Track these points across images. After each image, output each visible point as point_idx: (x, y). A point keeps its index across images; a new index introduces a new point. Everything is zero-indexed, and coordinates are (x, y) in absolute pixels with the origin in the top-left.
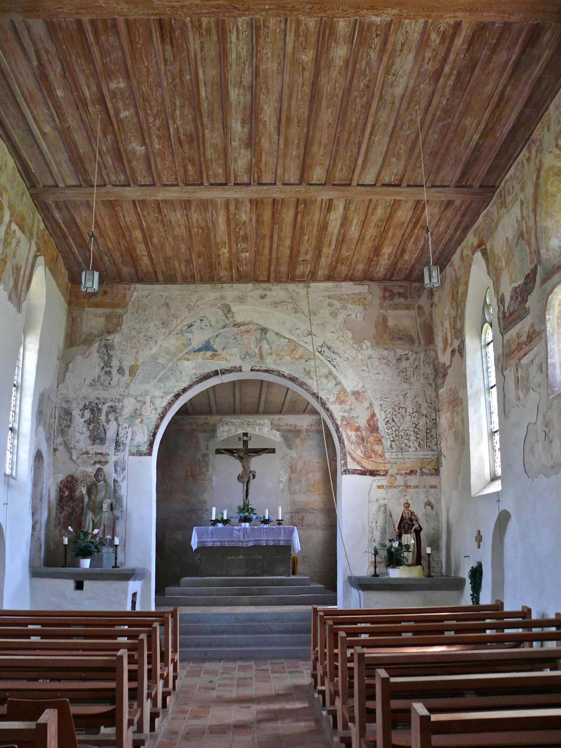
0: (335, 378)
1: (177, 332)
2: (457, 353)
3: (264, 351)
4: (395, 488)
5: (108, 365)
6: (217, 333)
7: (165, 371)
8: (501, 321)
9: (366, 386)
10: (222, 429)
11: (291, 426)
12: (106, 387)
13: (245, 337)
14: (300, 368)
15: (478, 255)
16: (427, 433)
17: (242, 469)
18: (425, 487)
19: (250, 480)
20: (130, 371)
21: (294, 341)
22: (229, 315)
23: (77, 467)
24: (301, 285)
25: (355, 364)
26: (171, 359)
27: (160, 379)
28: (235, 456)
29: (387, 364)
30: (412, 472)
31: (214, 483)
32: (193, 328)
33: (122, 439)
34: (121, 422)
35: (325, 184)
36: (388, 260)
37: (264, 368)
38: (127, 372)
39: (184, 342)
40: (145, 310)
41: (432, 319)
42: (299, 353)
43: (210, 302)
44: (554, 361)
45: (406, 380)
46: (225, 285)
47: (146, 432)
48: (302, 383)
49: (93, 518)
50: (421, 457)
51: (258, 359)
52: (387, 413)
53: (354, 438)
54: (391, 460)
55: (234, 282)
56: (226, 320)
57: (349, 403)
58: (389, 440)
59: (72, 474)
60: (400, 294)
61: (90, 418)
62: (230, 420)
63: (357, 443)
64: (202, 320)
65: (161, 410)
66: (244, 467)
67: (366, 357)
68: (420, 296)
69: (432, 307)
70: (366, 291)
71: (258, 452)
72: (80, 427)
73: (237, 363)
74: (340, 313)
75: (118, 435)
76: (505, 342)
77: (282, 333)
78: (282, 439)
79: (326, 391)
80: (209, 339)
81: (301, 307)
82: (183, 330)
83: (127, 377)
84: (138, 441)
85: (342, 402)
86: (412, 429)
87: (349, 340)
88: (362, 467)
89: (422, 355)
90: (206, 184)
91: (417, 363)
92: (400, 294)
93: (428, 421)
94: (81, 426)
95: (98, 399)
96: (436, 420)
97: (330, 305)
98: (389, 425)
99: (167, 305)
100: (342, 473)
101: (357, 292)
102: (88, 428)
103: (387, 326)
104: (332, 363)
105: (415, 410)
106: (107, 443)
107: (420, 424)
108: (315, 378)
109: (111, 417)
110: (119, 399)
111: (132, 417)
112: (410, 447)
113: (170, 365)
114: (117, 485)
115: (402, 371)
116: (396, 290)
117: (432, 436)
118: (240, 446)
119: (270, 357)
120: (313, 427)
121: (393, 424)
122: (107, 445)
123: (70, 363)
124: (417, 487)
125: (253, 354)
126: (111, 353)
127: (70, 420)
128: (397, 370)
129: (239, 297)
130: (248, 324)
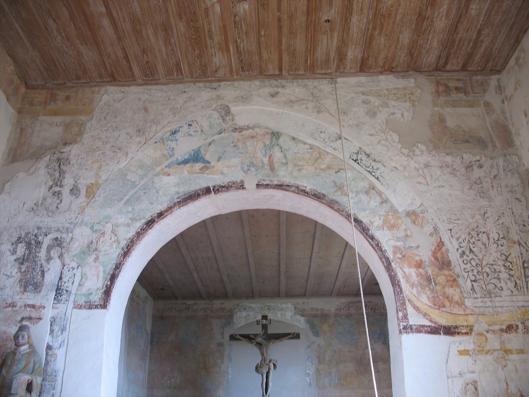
0: (380, 194)
1: (156, 140)
4: (487, 353)
5: (59, 183)
6: (210, 140)
7: (135, 190)
10: (239, 314)
11: (317, 310)
13: (248, 143)
22: (227, 118)
24: (325, 81)
27: (128, 201)
29: (454, 172)
30: (510, 328)
31: (230, 376)
32: (178, 135)
33: (67, 284)
34: (67, 260)
36: (447, 16)
37: (276, 183)
38: (83, 192)
39: (165, 152)
41: (506, 118)
45: (482, 194)
46: (222, 83)
47: (101, 274)
48: (331, 201)
50: (521, 304)
52: (461, 240)
53: (414, 278)
54: (474, 309)
55: (235, 77)
56: (224, 125)
57: (403, 227)
58: (469, 280)
60: (457, 89)
61: (24, 255)
62: (248, 305)
63: (421, 285)
65: (125, 242)
66: (262, 354)
68: (485, 91)
69: (503, 102)
71: (278, 337)
73: (237, 176)
74: (380, 112)
75: (61, 278)
77: (301, 138)
78: (308, 326)
79: (368, 212)
80: (200, 147)
81: (326, 106)
82: (164, 137)
83: (82, 199)
84: (88, 288)
85: (392, 227)
86: (501, 263)
87: (395, 144)
88: (431, 321)
89: (501, 161)
91: (494, 172)
92: (457, 89)
94: (10, 265)
95: (39, 228)
98: (465, 257)
99: (146, 109)
100: (400, 332)
102: (20, 268)
103: (446, 126)
104: (373, 174)
105: (501, 236)
106: (43, 290)
107: (513, 255)
108: (350, 194)
109: (54, 253)
110: (67, 228)
111: (83, 253)
113: (143, 182)
114: (50, 353)
115: (476, 183)
116: (452, 84)
118: (258, 330)
119: (284, 168)
120: (342, 312)
121: (471, 256)
122: (43, 293)
123: (8, 182)
125: (260, 164)
128: (468, 182)
130: (253, 128)
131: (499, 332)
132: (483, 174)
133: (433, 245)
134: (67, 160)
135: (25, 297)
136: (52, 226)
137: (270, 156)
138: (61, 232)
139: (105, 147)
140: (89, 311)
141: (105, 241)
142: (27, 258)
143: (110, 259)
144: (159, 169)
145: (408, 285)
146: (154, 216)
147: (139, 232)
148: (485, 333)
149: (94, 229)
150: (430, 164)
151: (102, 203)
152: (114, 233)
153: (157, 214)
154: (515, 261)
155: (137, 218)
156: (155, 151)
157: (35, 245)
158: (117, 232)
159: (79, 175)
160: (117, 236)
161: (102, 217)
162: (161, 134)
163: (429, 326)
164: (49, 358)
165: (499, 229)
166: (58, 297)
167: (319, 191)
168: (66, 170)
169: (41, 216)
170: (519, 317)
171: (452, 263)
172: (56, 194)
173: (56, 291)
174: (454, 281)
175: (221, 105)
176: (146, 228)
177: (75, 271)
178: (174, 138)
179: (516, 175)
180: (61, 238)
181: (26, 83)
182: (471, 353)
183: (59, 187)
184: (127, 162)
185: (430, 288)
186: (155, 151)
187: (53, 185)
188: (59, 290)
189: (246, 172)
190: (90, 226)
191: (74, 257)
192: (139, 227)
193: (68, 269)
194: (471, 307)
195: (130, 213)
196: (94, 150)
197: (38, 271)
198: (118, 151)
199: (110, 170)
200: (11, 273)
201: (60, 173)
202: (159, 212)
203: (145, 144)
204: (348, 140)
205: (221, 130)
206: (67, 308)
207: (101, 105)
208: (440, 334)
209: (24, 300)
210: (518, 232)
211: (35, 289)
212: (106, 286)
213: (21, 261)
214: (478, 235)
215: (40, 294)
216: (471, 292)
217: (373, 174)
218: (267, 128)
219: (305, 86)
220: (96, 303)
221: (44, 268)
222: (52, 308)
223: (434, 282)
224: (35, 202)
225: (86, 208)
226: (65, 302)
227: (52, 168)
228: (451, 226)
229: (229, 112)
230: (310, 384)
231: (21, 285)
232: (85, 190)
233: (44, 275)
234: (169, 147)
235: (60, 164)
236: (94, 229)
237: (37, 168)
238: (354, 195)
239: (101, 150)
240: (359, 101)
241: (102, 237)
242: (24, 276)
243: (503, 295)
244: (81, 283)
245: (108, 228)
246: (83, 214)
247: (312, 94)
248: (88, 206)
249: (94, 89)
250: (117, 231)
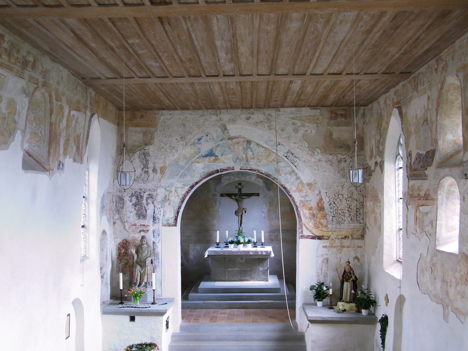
0: (296, 174)
2: (379, 166)
3: (249, 156)
4: (334, 247)
5: (146, 167)
6: (217, 144)
7: (184, 170)
8: (409, 169)
9: (316, 180)
12: (145, 181)
14: (273, 167)
15: (396, 111)
16: (357, 211)
17: (237, 207)
18: (354, 247)
19: (243, 214)
20: (160, 171)
21: (269, 149)
22: (225, 132)
23: (129, 234)
24: (274, 110)
25: (310, 165)
26: (187, 163)
27: (181, 176)
28: (233, 199)
29: (331, 165)
30: (346, 237)
32: (202, 141)
34: (156, 205)
35: (287, 75)
37: (249, 168)
38: (159, 171)
39: (196, 150)
40: (169, 128)
41: (363, 133)
42: (272, 157)
43: (212, 123)
44: (442, 223)
45: (344, 176)
46: (222, 111)
47: (173, 211)
49: (141, 271)
50: (352, 227)
51: (244, 162)
52: (330, 198)
53: (308, 215)
56: (224, 136)
57: (305, 191)
58: (331, 216)
59: (125, 238)
60: (341, 115)
63: (310, 218)
64: (207, 135)
65: (182, 196)
66: (239, 206)
67: (317, 160)
69: (364, 124)
70: (319, 114)
72: (130, 208)
73: (231, 164)
74: (300, 130)
75: (154, 213)
76: (410, 186)
78: (264, 184)
79: (290, 183)
80: (212, 148)
83: (159, 175)
85: (300, 191)
86: (347, 209)
88: (313, 234)
90: (203, 76)
92: (341, 115)
93: (358, 203)
94: (130, 207)
95: (141, 189)
96: (363, 202)
97: (293, 124)
98: (331, 206)
99: (184, 125)
100: (299, 238)
101: (312, 114)
102: (135, 208)
103: (332, 138)
104: (294, 164)
105: (349, 196)
106: (147, 218)
107: (352, 206)
108: (282, 175)
109: (150, 201)
110: (154, 189)
111: (163, 201)
112: (345, 221)
113: (187, 166)
115: (341, 170)
116: (339, 112)
117: (360, 213)
119: (252, 161)
121: (334, 205)
122: (147, 219)
124: (349, 247)
125: (242, 158)
128: (338, 169)
129: (232, 119)
131: (341, 239)
132: (346, 165)
133: (318, 200)
137: (246, 154)
144: (194, 159)
145: (304, 218)
148: (335, 239)
149: (167, 189)
150: (321, 160)
151: (168, 176)
154: (353, 208)
163: (312, 236)
164: (154, 247)
165: (348, 193)
167: (268, 173)
170: (350, 232)
171: (325, 208)
174: (324, 217)
175: (222, 124)
177: (160, 209)
179: (361, 166)
182: (327, 247)
185: (314, 220)
188: (154, 218)
189: (235, 163)
190: (164, 188)
194: (331, 228)
198: (173, 149)
199: (171, 159)
204: (283, 145)
205: (222, 139)
208: (316, 239)
210: (357, 194)
211: (144, 218)
213: (135, 205)
214: (338, 195)
216: (331, 221)
217: (294, 164)
218: (245, 138)
219: (264, 113)
223: (316, 217)
228: (327, 191)
229: (226, 128)
230: (265, 218)
231: (137, 216)
232: (159, 170)
235: (145, 156)
238: (284, 175)
240: (290, 123)
243: (345, 223)
245: (173, 189)
247: (267, 118)
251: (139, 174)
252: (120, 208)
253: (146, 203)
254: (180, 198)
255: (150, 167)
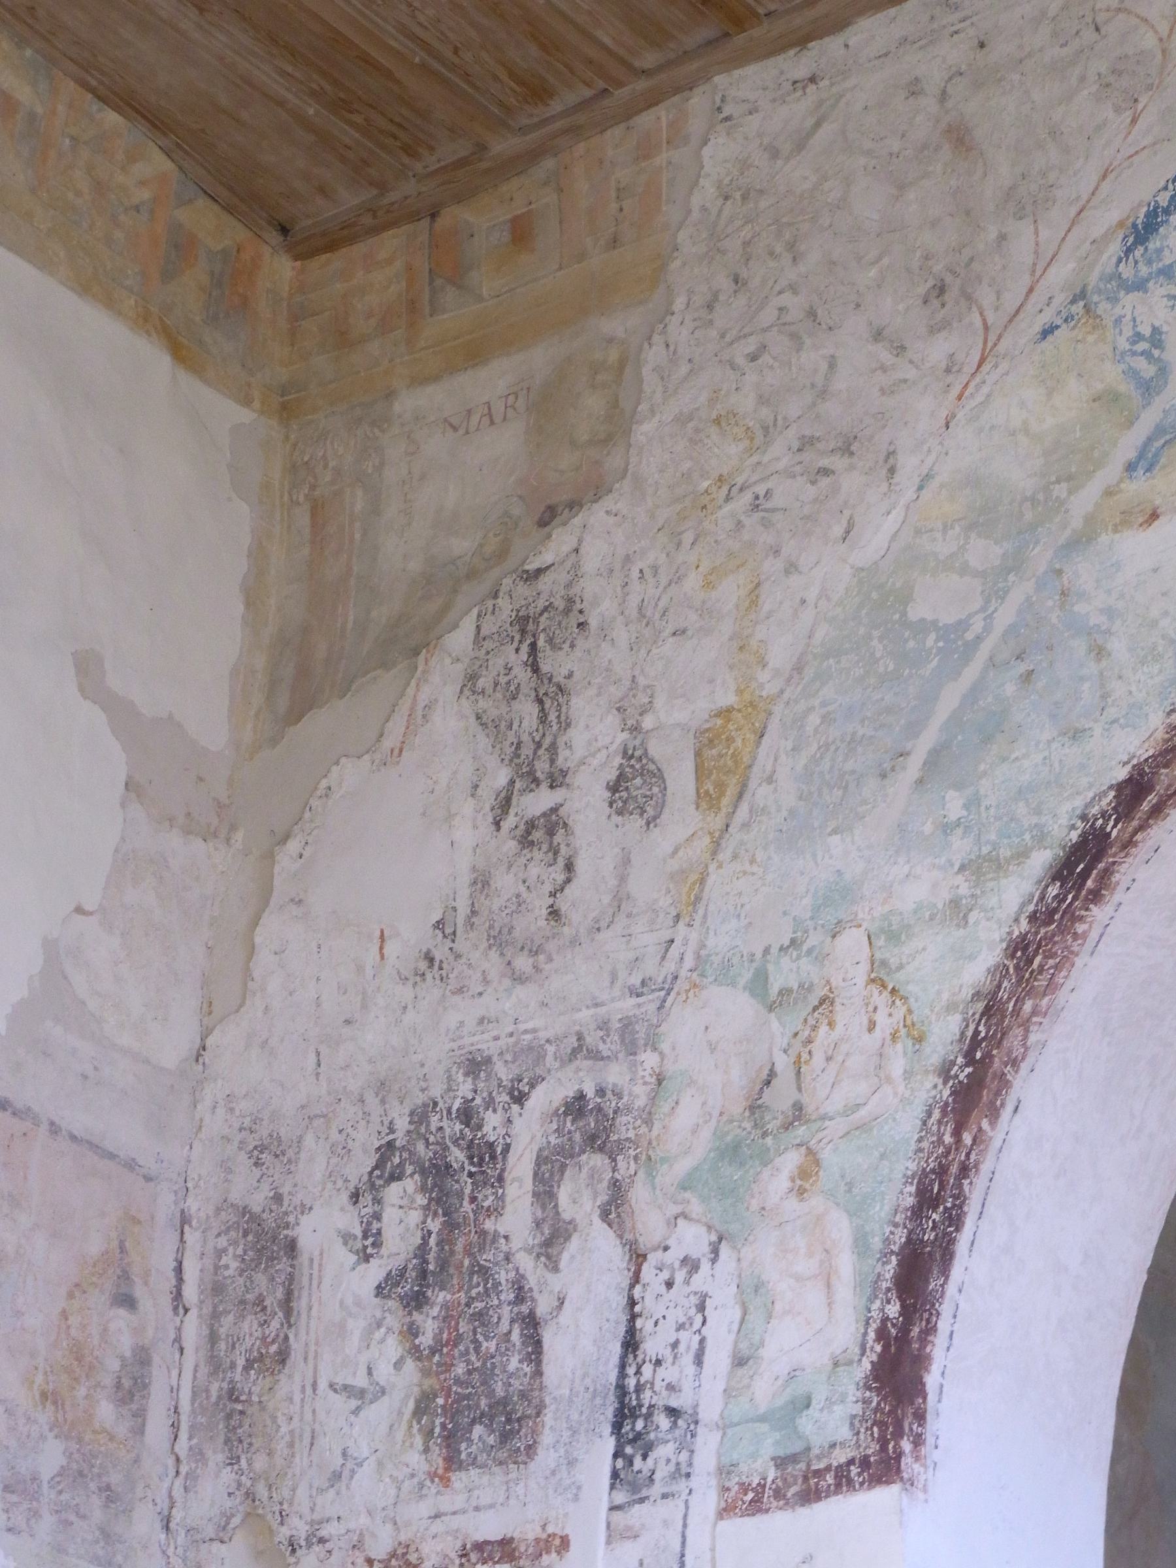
7: (971, 673)
20: (701, 772)
26: (1014, 564)
33: (667, 1373)
39: (1111, 375)
40: (791, 246)
47: (846, 1264)
61: (423, 1247)
65: (954, 1023)
75: (631, 1343)
82: (1093, 279)
84: (782, 1368)
95: (476, 1065)
102: (412, 1331)
106: (547, 1438)
110: (627, 1024)
113: (1005, 615)
122: (546, 1458)
126: (555, 663)
127: (287, 1305)
134: (567, 611)
135: (459, 1501)
136: (543, 1035)
138: (595, 1055)
139: (766, 459)
140: (804, 1512)
141: (844, 1048)
142: (438, 1258)
143: (883, 1156)
146: (1095, 810)
147: (1023, 937)
149: (774, 990)
151: (792, 812)
152: (884, 986)
153: (1112, 794)
155: (1005, 852)
156: (1050, 394)
157: (471, 1175)
158: (901, 976)
159: (642, 681)
160: (904, 999)
161: (805, 901)
162: (1071, 265)
166: (631, 1464)
168: (570, 676)
169: (480, 989)
172: (537, 835)
173: (617, 1427)
176: (1061, 899)
177: (700, 1281)
178: (1149, 262)
180: (601, 1092)
181: (284, 230)
183: (544, 786)
184: (897, 515)
186: (1050, 394)
187: (512, 782)
190: (747, 975)
191: (687, 1195)
192: (1023, 905)
193: (665, 1275)
195: (959, 831)
196: (705, 500)
197: (504, 1326)
198: (838, 463)
199: (812, 595)
200: (370, 1372)
201: (540, 702)
202: (1122, 774)
203: (986, 367)
206: (685, 1526)
207: (704, 209)
209: (455, 1522)
211: (505, 1437)
212: (882, 1334)
215: (532, 1466)
220: (840, 1457)
221: (533, 1300)
222: (608, 1542)
224: (437, 916)
225: (712, 867)
226: (674, 1488)
227: (496, 684)
231: (429, 1434)
232: (688, 765)
233: (538, 1344)
234: (1128, 332)
235: (533, 646)
236: (774, 990)
237: (420, 713)
239: (741, 490)
241: (823, 1029)
242: (438, 1374)
244: (743, 1346)
246: (701, 912)
248: (721, 857)
249: (645, 120)
250: (901, 967)
251: (465, 878)
252: (248, 1367)
253: (538, 1224)
254: (935, 1060)
255: (579, 753)
